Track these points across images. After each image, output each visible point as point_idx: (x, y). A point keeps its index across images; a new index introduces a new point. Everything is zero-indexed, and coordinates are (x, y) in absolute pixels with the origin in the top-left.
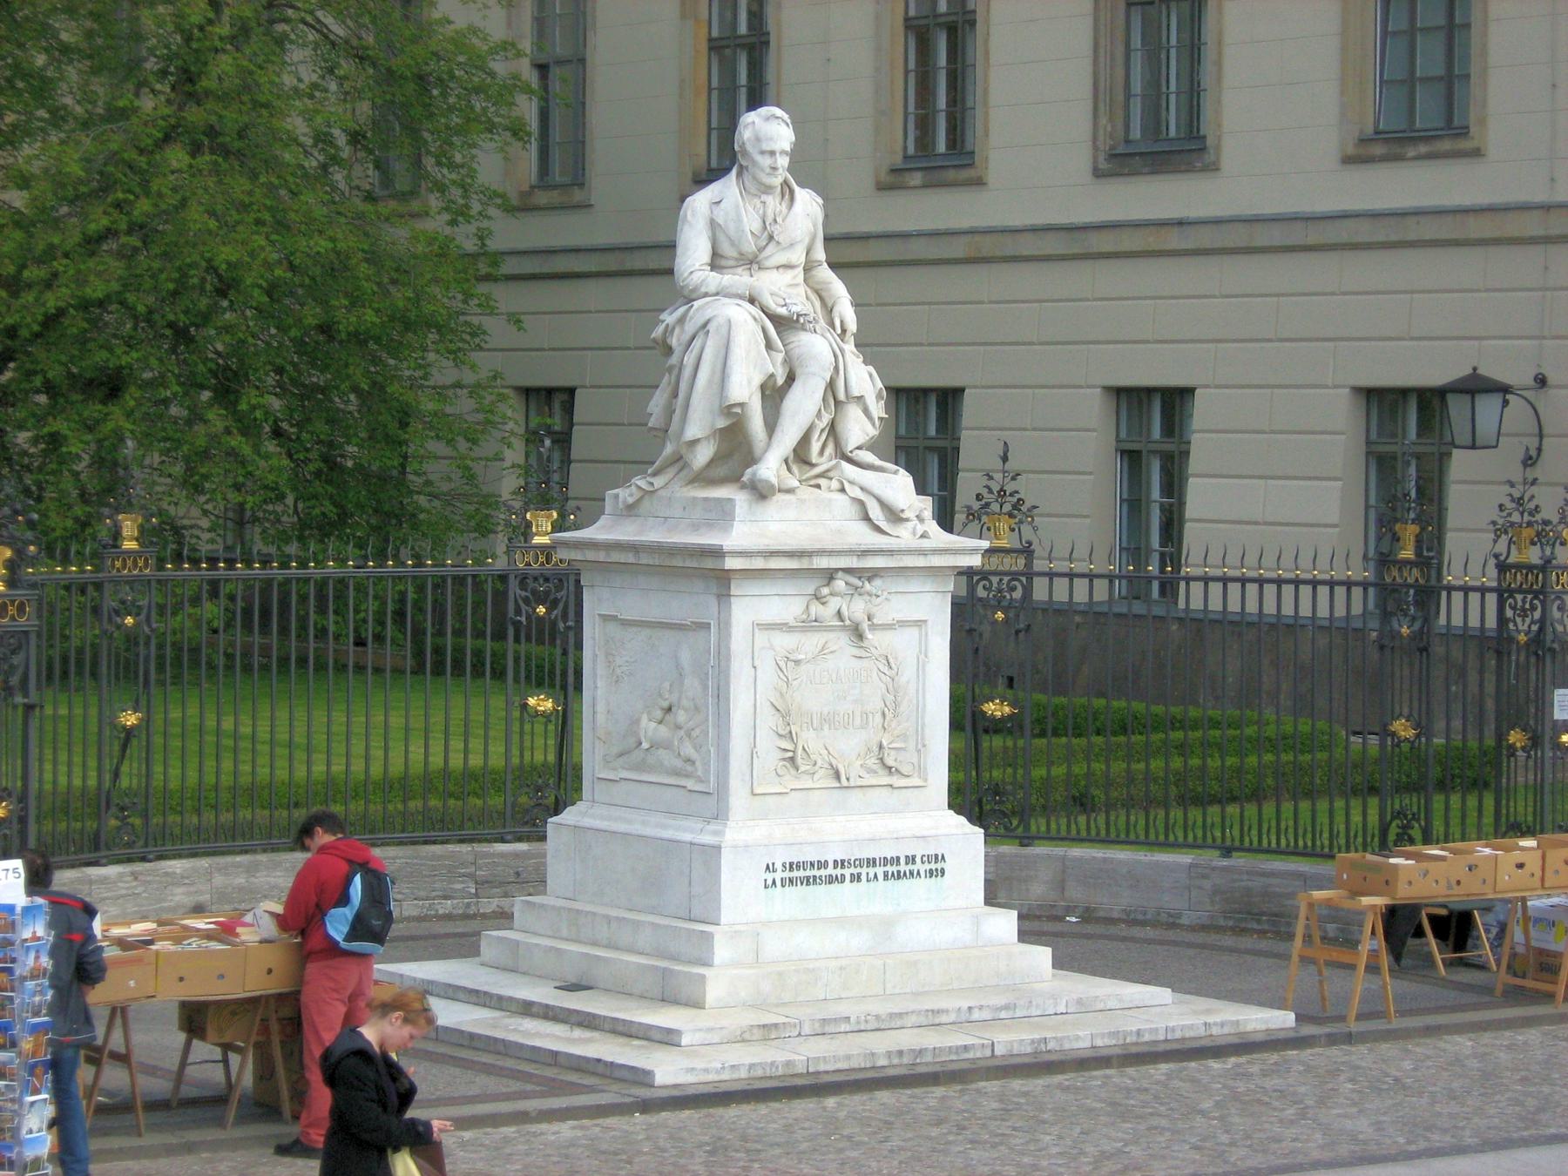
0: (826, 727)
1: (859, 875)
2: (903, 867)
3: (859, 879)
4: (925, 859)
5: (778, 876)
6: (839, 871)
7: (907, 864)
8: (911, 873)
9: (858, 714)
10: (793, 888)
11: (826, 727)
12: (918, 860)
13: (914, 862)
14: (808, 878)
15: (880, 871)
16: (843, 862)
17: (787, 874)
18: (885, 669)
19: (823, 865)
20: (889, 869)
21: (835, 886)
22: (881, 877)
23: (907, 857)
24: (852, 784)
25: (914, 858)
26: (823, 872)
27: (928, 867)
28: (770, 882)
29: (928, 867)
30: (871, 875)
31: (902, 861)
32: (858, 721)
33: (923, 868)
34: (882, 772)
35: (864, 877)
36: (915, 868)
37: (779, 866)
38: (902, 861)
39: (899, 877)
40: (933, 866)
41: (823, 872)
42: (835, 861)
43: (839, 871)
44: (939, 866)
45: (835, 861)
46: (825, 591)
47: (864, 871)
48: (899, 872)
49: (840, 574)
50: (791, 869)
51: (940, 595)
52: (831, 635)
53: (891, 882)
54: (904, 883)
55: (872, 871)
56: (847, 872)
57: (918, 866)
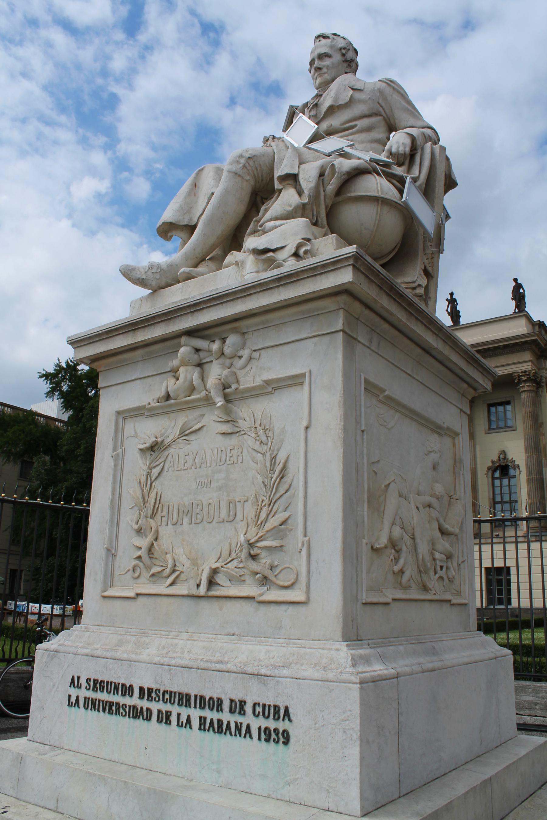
0: (186, 520)
1: (169, 714)
2: (226, 716)
3: (168, 721)
4: (259, 709)
5: (84, 693)
6: (145, 704)
7: (232, 711)
8: (238, 727)
9: (224, 503)
10: (94, 713)
11: (186, 520)
12: (248, 709)
13: (242, 712)
14: (111, 704)
15: (195, 714)
16: (150, 690)
17: (90, 694)
18: (257, 446)
19: (128, 690)
20: (210, 715)
21: (140, 722)
22: (195, 723)
23: (232, 701)
24: (202, 590)
25: (242, 703)
26: (127, 701)
27: (263, 723)
28: (73, 700)
29: (263, 723)
30: (184, 719)
31: (226, 706)
32: (224, 514)
33: (256, 723)
34: (249, 579)
35: (174, 718)
36: (244, 721)
37: (83, 681)
38: (226, 706)
39: (220, 730)
40: (271, 724)
41: (127, 701)
42: (141, 689)
43: (145, 704)
44: (281, 725)
45: (141, 689)
46: (175, 362)
47: (175, 709)
48: (220, 722)
49: (183, 339)
50: (95, 689)
51: (326, 339)
52: (196, 413)
53: (210, 735)
54: (226, 740)
55: (185, 712)
56: (155, 706)
57: (248, 719)
